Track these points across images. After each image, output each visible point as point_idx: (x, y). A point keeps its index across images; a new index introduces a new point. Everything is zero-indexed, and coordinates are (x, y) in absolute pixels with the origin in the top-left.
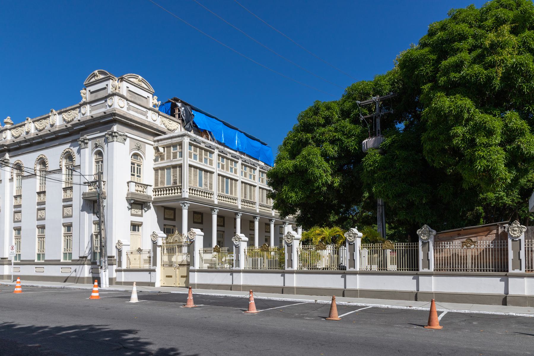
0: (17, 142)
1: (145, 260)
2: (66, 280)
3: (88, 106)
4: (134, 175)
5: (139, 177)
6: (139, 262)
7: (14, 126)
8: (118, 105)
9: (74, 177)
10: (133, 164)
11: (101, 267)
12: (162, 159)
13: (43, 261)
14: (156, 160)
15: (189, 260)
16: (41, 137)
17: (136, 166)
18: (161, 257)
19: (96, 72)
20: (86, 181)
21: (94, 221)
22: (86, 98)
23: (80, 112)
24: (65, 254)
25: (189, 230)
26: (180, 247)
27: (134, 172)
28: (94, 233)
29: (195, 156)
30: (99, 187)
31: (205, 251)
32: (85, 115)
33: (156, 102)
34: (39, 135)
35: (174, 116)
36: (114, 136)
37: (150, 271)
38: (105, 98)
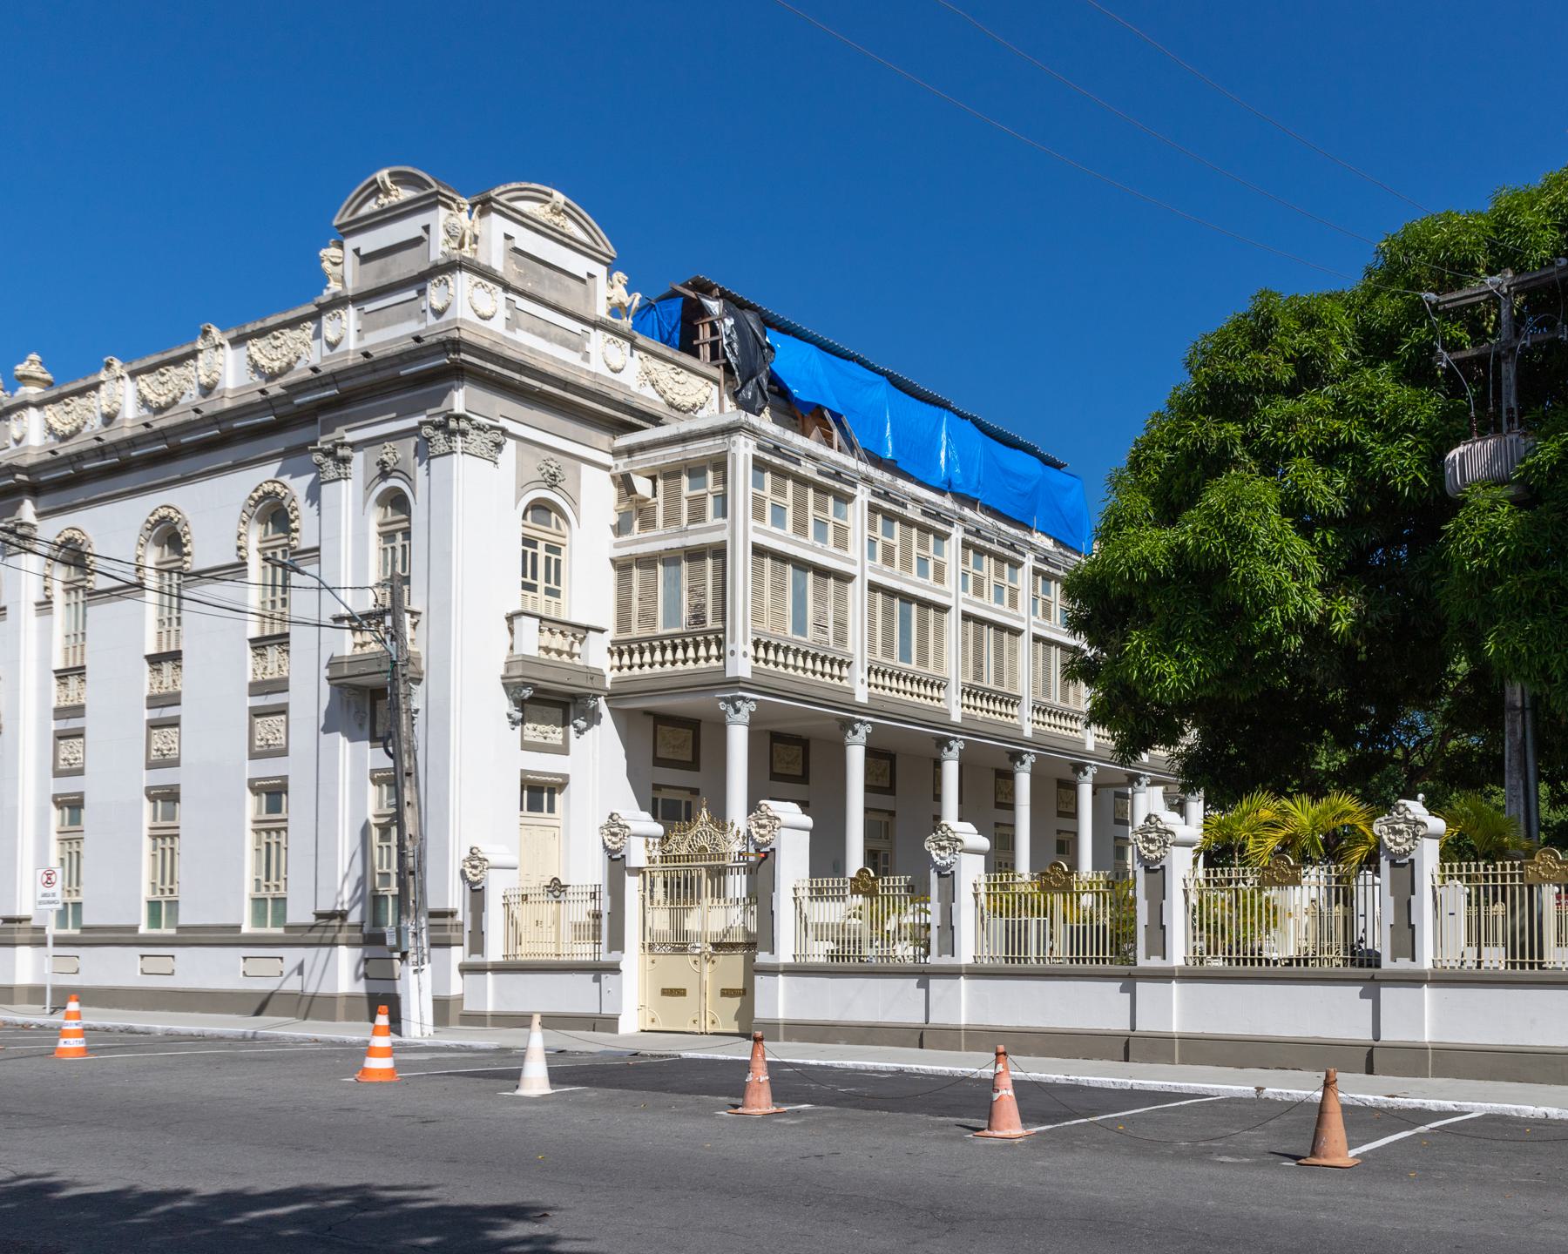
0: (68, 457)
1: (577, 927)
2: (263, 1004)
3: (352, 310)
4: (533, 588)
5: (556, 594)
6: (556, 933)
7: (54, 392)
8: (471, 308)
9: (295, 596)
10: (529, 542)
11: (404, 956)
12: (648, 523)
13: (172, 932)
14: (620, 529)
15: (753, 928)
16: (162, 434)
17: (541, 551)
18: (643, 913)
19: (383, 175)
20: (344, 612)
21: (373, 771)
22: (343, 281)
23: (317, 335)
24: (259, 902)
25: (753, 807)
26: (719, 873)
27: (534, 576)
28: (373, 820)
29: (778, 510)
30: (396, 634)
31: (819, 890)
32: (337, 350)
34: (156, 426)
35: (695, 353)
36: (452, 433)
37: (598, 970)
38: (419, 281)
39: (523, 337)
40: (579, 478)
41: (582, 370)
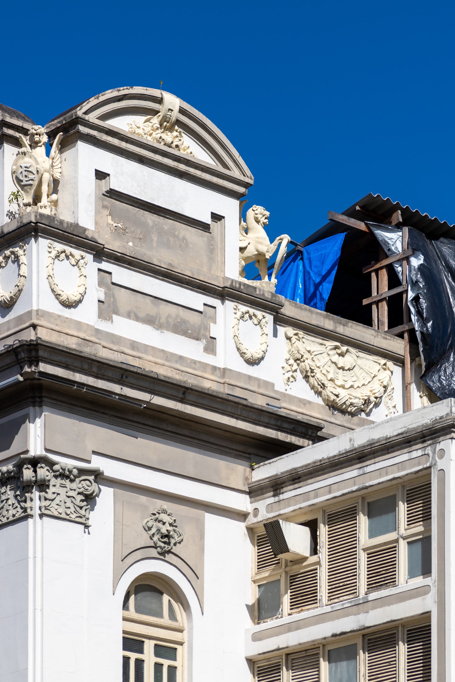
10: (132, 643)
14: (262, 609)
17: (149, 657)
33: (259, 241)
36: (27, 487)
39: (125, 328)
40: (202, 537)
41: (204, 366)
